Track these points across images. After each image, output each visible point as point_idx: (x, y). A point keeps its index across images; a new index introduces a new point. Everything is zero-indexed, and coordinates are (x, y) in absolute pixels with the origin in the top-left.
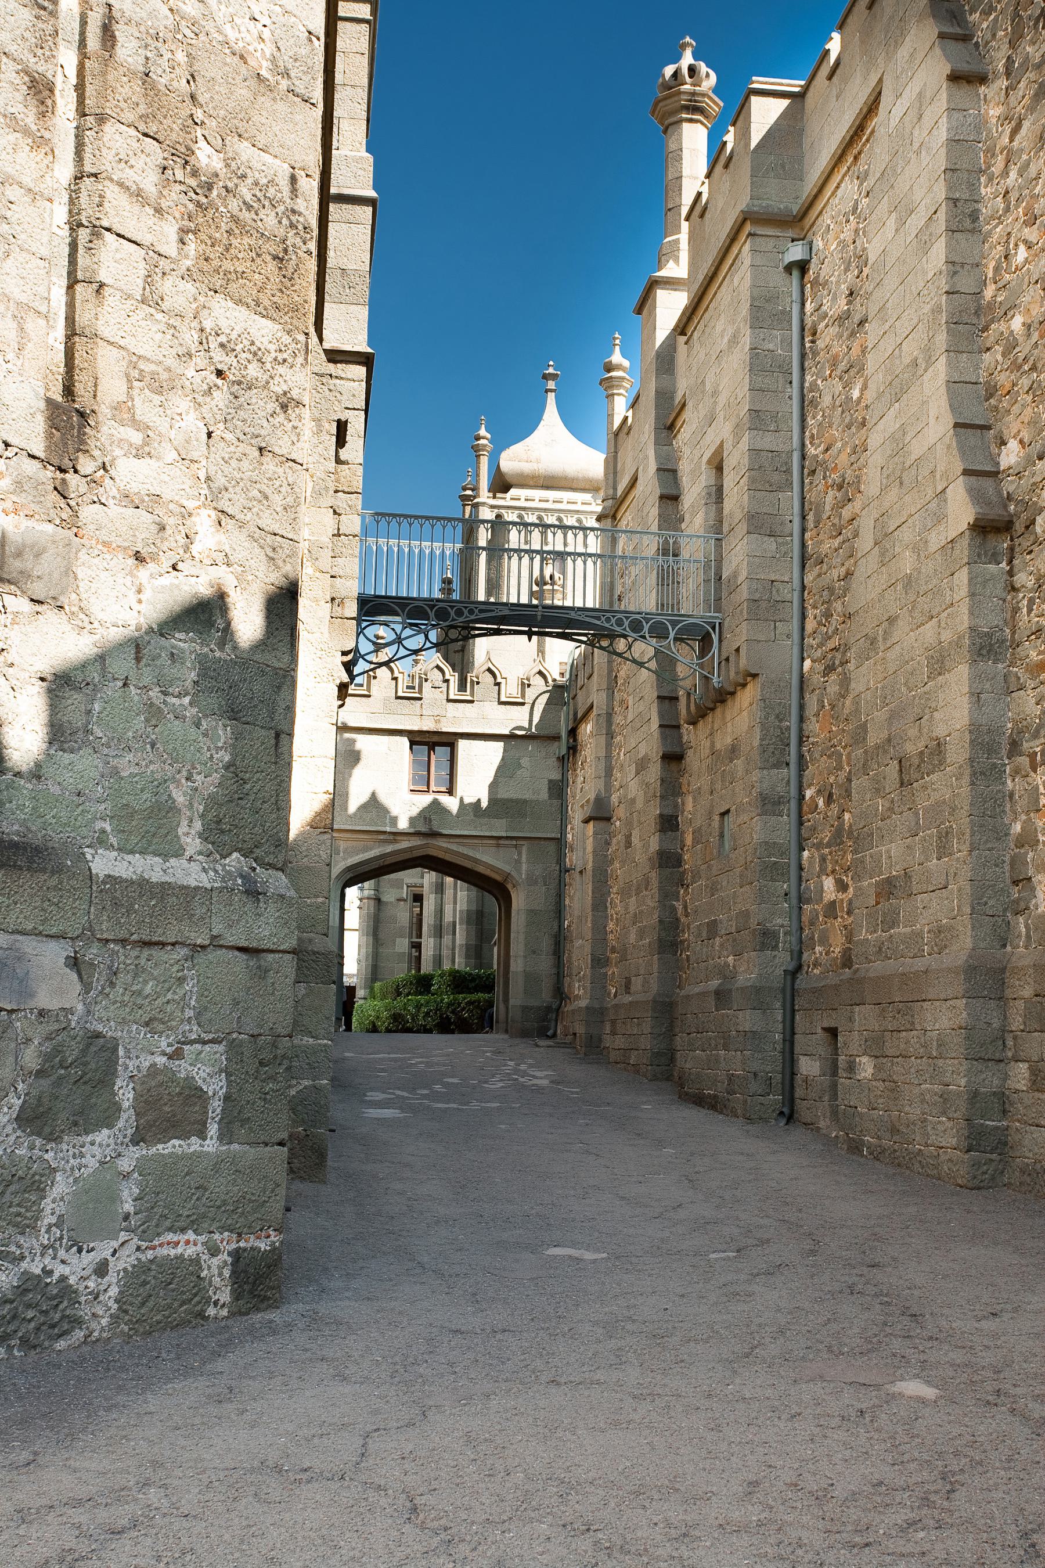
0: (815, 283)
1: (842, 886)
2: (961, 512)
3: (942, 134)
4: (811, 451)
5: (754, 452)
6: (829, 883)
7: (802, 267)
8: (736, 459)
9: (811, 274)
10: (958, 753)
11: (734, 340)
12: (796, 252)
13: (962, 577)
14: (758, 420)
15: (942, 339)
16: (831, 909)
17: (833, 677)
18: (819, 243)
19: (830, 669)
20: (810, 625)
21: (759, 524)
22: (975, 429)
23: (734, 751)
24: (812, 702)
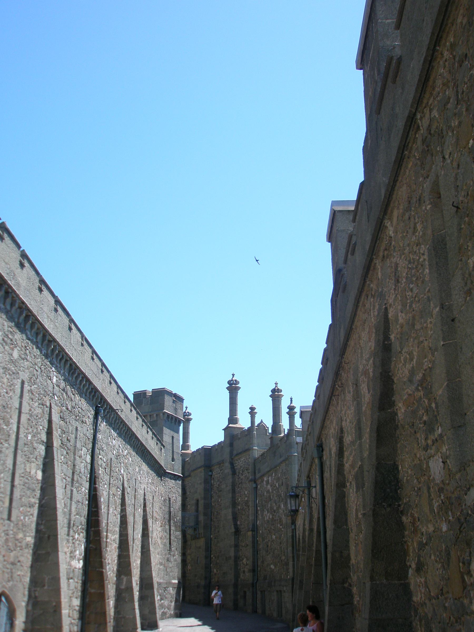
0: (213, 478)
1: (217, 571)
2: (233, 530)
3: (231, 480)
4: (212, 504)
5: (204, 503)
6: (215, 570)
7: (211, 476)
8: (201, 503)
9: (213, 477)
10: (233, 558)
11: (201, 484)
12: (210, 473)
13: (233, 537)
14: (205, 498)
15: (231, 506)
16: (215, 574)
17: (216, 540)
18: (214, 473)
19: (215, 538)
20: (212, 531)
21: (205, 514)
22: (235, 518)
23: (200, 548)
24: (213, 542)
